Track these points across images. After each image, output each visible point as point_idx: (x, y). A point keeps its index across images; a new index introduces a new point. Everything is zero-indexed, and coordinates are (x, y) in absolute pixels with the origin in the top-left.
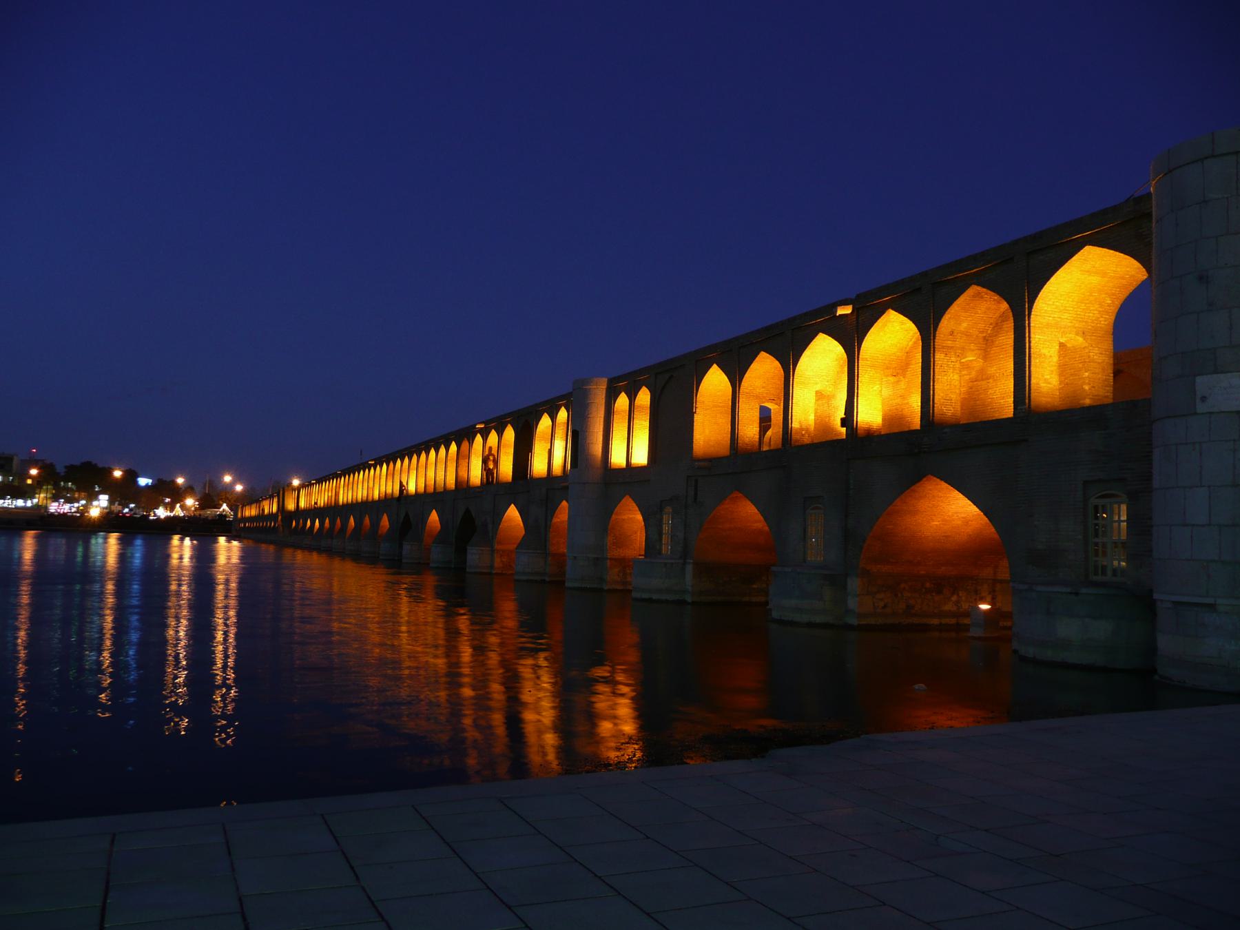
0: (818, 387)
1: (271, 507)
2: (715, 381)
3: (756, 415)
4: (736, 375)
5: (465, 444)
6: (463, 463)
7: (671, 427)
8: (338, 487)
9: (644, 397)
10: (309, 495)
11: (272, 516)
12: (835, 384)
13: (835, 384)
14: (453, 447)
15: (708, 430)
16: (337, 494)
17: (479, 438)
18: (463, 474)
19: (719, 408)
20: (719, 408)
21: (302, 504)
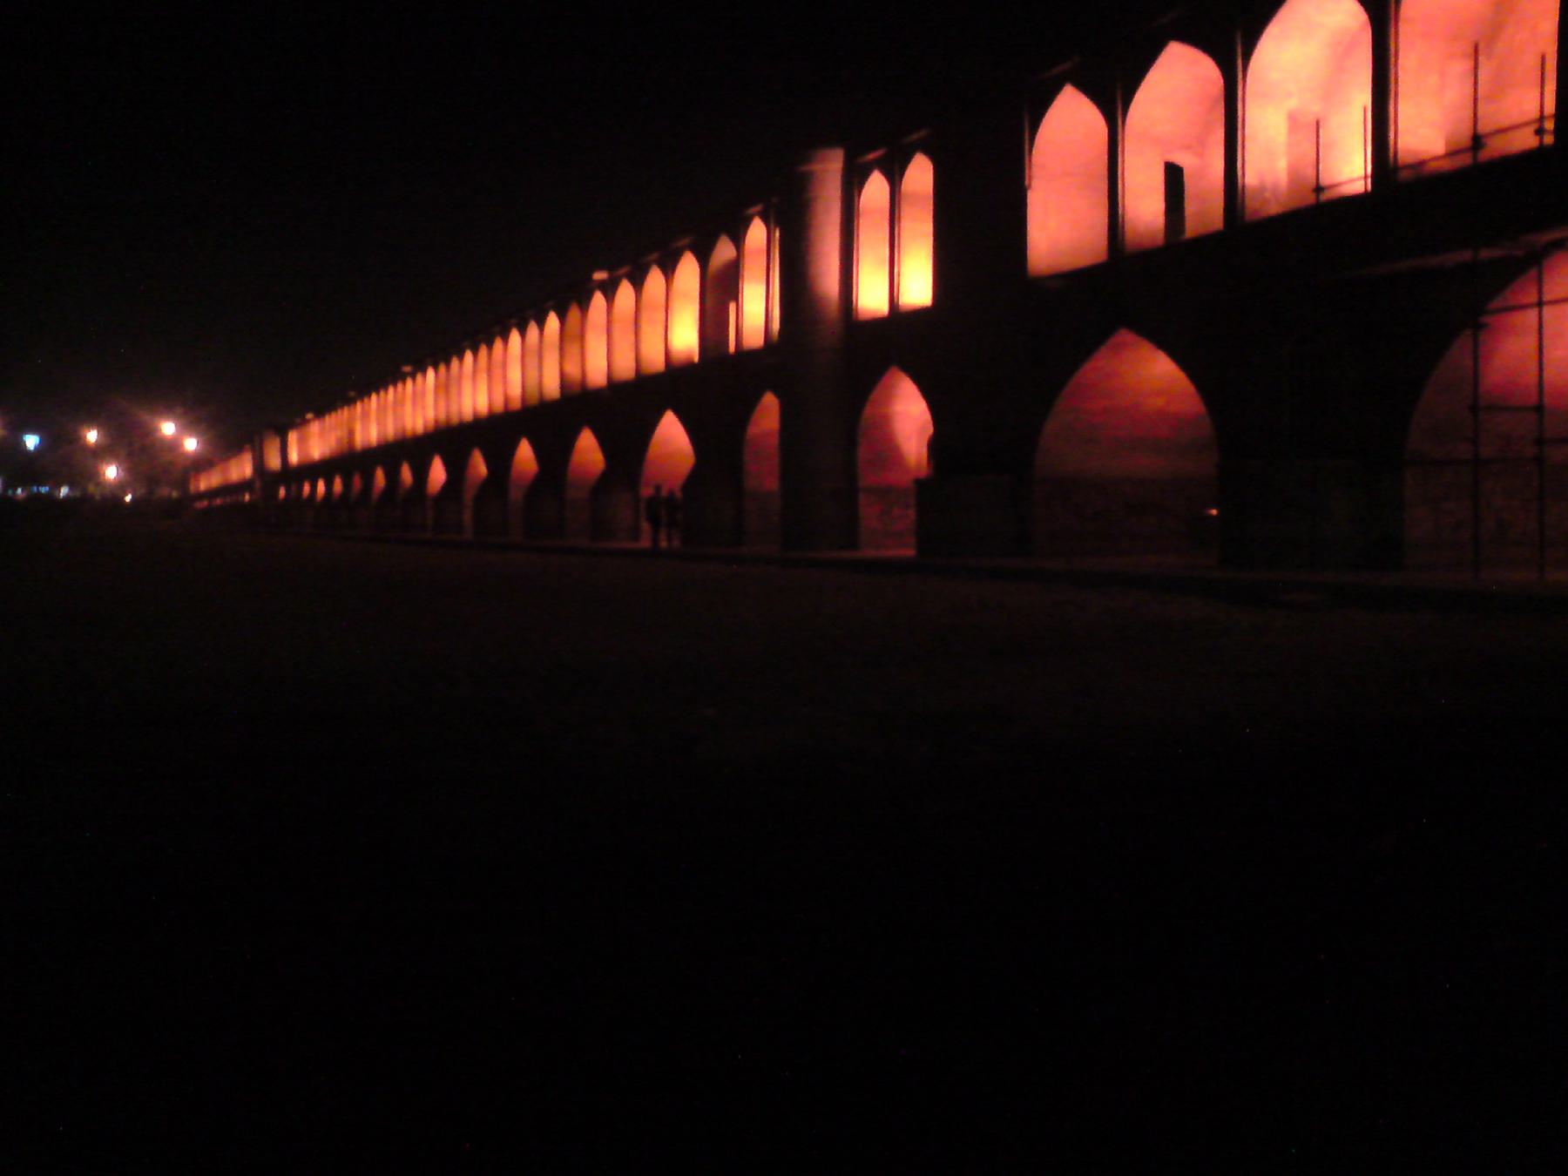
0: (1293, 103)
1: (242, 468)
2: (1070, 119)
3: (1158, 178)
4: (1113, 99)
5: (574, 314)
6: (572, 350)
7: (980, 224)
8: (351, 420)
9: (920, 174)
10: (302, 441)
11: (244, 485)
12: (1331, 90)
13: (1331, 90)
14: (553, 322)
15: (1059, 225)
16: (351, 433)
17: (598, 299)
18: (573, 370)
19: (1081, 181)
20: (1081, 181)
21: (294, 457)
